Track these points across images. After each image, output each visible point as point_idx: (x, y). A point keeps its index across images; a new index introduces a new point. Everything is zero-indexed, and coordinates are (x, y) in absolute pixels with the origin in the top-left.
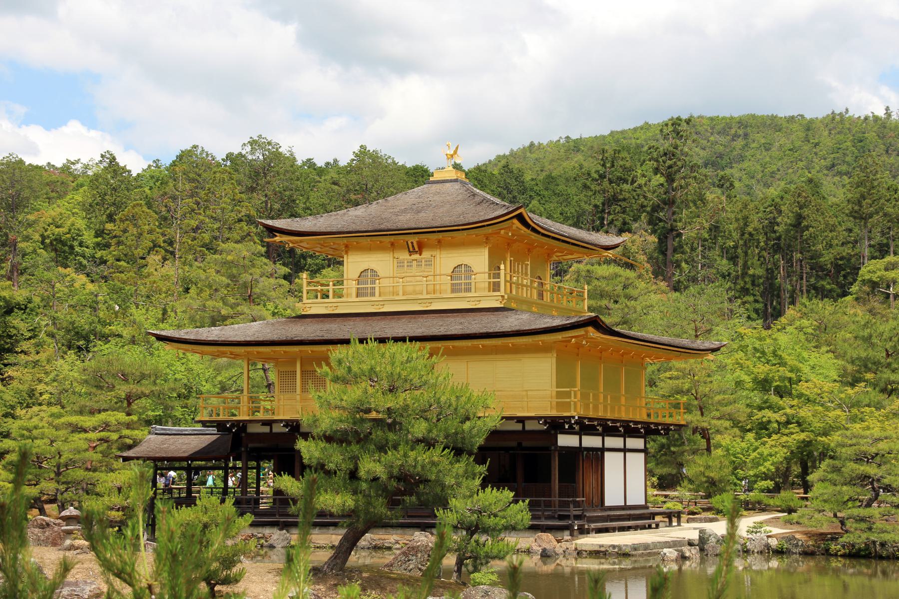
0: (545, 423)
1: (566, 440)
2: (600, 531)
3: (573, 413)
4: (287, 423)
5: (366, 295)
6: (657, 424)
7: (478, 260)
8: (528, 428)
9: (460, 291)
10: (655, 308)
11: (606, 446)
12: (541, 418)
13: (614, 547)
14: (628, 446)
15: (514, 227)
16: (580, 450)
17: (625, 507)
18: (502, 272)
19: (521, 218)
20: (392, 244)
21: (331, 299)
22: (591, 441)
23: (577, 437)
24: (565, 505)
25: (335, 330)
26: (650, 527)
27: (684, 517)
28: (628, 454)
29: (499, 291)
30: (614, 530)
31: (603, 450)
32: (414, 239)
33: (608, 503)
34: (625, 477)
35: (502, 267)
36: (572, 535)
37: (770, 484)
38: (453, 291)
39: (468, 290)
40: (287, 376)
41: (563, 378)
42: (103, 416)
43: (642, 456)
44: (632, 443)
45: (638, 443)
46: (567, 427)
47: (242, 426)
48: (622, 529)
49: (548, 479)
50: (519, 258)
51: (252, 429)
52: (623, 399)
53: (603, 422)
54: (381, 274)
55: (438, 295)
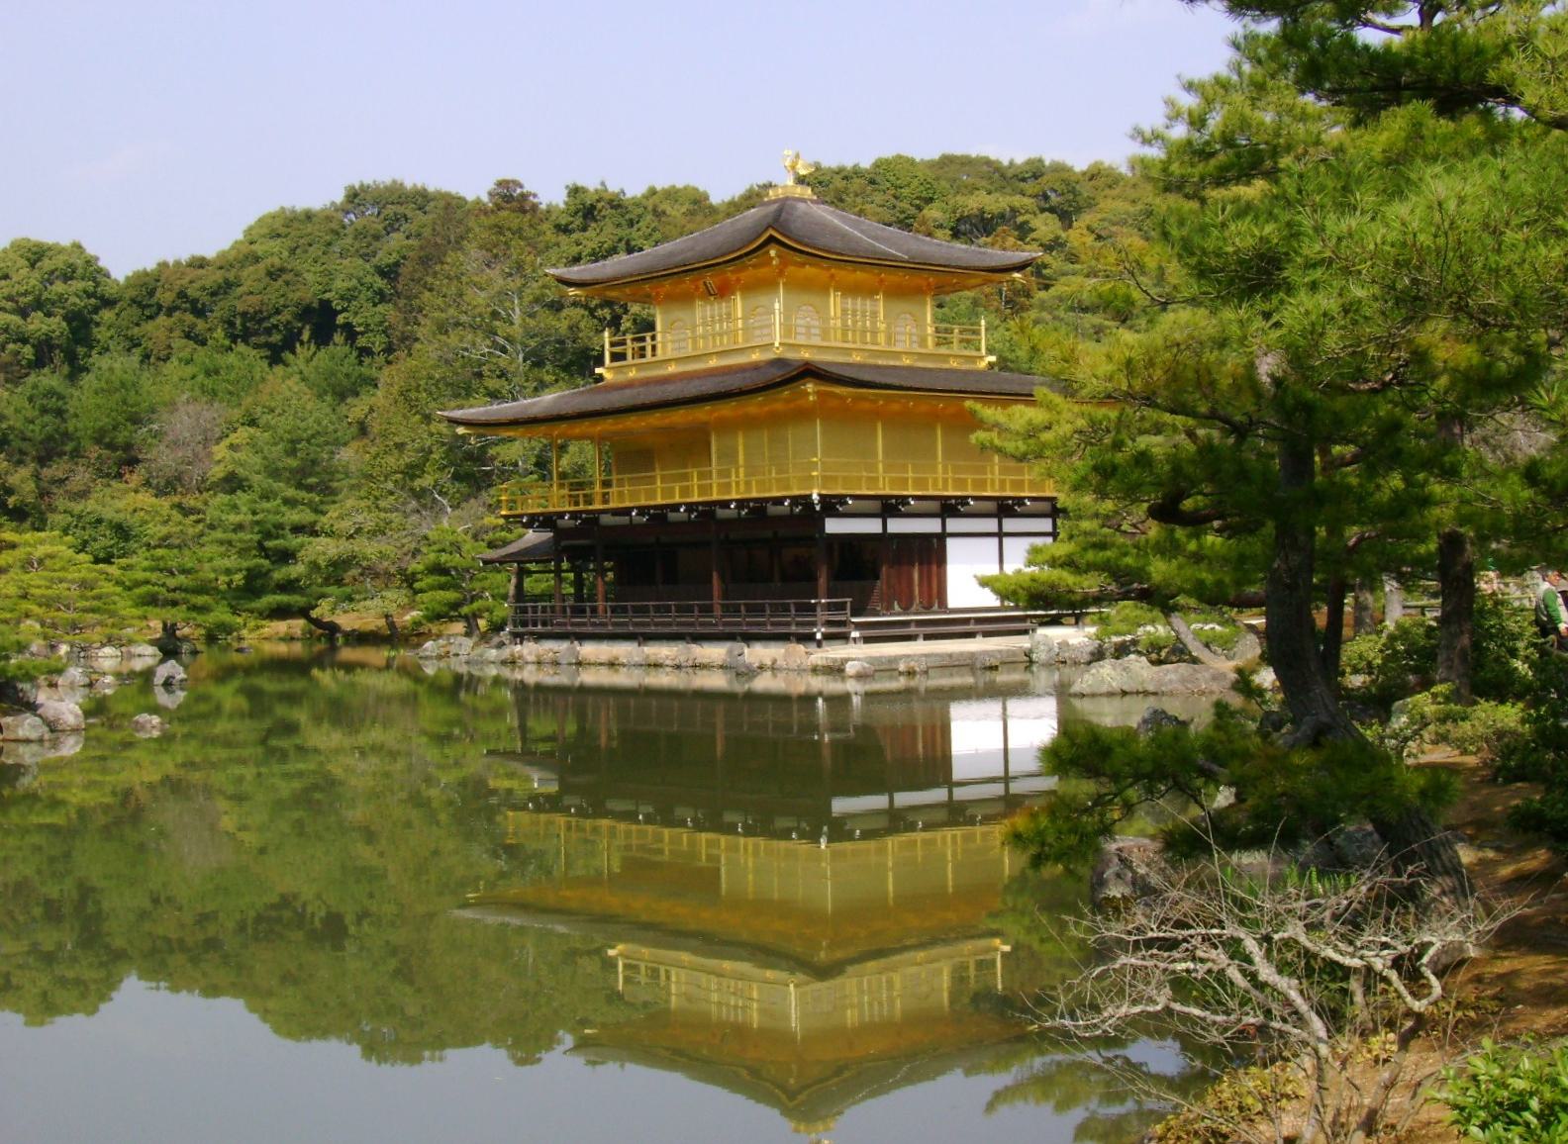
1: (833, 526)
2: (867, 640)
11: (949, 529)
15: (773, 253)
16: (884, 537)
21: (630, 360)
22: (896, 526)
26: (1025, 632)
28: (1006, 540)
31: (942, 537)
32: (711, 280)
33: (953, 601)
36: (819, 644)
44: (1009, 525)
46: (818, 508)
47: (546, 521)
48: (928, 637)
53: (904, 500)
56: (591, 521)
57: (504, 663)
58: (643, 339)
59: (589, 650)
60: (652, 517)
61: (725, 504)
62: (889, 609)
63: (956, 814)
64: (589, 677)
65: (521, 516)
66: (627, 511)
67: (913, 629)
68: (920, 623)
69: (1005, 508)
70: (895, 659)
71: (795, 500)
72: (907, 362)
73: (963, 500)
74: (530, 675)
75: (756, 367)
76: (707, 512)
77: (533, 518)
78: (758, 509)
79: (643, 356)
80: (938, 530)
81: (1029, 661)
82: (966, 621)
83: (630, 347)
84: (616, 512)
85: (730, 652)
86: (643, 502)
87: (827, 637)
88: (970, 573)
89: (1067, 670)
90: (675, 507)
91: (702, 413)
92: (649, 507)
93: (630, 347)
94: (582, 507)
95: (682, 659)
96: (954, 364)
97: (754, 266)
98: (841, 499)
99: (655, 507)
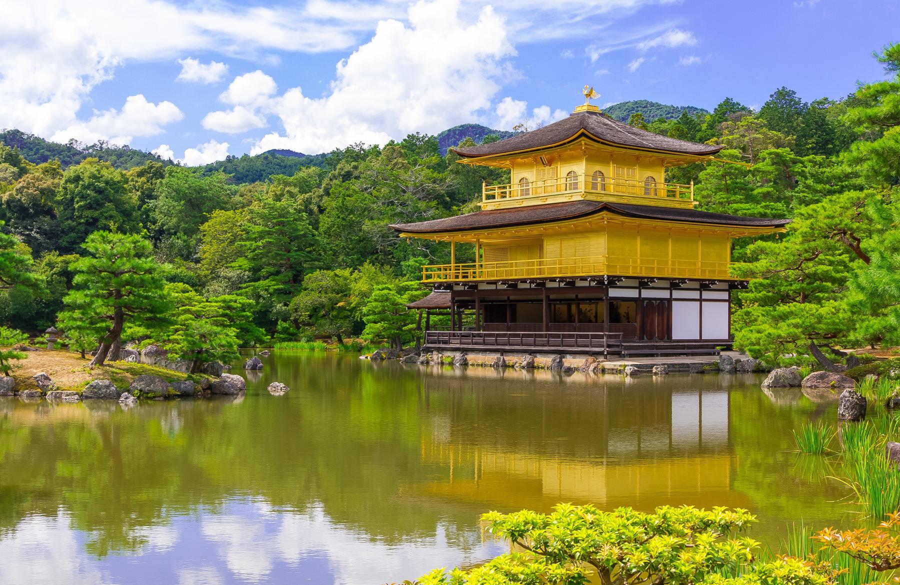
1: (613, 293)
2: (631, 356)
4: (465, 284)
15: (583, 142)
16: (638, 301)
17: (701, 340)
20: (536, 160)
22: (646, 294)
26: (714, 354)
30: (657, 355)
31: (670, 301)
32: (545, 156)
33: (675, 336)
44: (706, 295)
45: (725, 296)
47: (449, 286)
48: (663, 355)
51: (456, 288)
53: (652, 279)
54: (530, 180)
56: (474, 286)
57: (422, 363)
58: (505, 188)
59: (471, 357)
60: (510, 286)
61: (553, 280)
62: (641, 339)
63: (673, 452)
64: (471, 372)
65: (434, 283)
66: (495, 283)
67: (655, 351)
68: (657, 348)
70: (652, 366)
71: (593, 278)
72: (653, 204)
73: (683, 281)
74: (436, 370)
75: (572, 203)
76: (541, 283)
77: (440, 286)
78: (571, 283)
79: (505, 197)
81: (718, 370)
82: (684, 347)
83: (497, 192)
84: (489, 283)
85: (554, 360)
86: (505, 278)
87: (609, 353)
88: (685, 322)
89: (739, 375)
90: (524, 281)
91: (541, 228)
92: (508, 280)
93: (497, 192)
94: (469, 279)
95: (525, 363)
96: (678, 206)
97: (571, 150)
98: (619, 278)
99: (511, 280)
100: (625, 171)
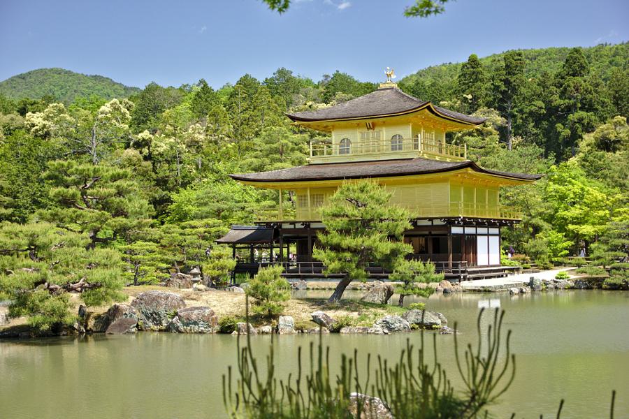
0: (444, 221)
1: (456, 230)
2: (475, 279)
3: (460, 216)
4: (303, 223)
5: (343, 153)
6: (506, 220)
7: (406, 132)
8: (434, 223)
9: (396, 149)
10: (504, 156)
11: (478, 233)
12: (441, 218)
13: (483, 287)
14: (490, 233)
16: (463, 235)
18: (419, 138)
19: (429, 108)
21: (325, 155)
23: (462, 228)
24: (455, 265)
25: (329, 171)
26: (502, 276)
27: (521, 272)
28: (490, 237)
29: (417, 149)
31: (476, 235)
32: (370, 121)
33: (479, 264)
34: (488, 251)
35: (419, 135)
37: (567, 252)
38: (392, 149)
39: (400, 149)
40: (302, 198)
41: (455, 197)
42: (206, 220)
43: (498, 237)
44: (492, 231)
45: (496, 231)
46: (456, 222)
47: (279, 225)
48: (487, 278)
49: (446, 251)
50: (428, 130)
52: (487, 207)
54: (352, 141)
55: (382, 152)
67: (480, 275)
69: (490, 224)
80: (474, 232)
82: (491, 271)
100: (428, 135)
